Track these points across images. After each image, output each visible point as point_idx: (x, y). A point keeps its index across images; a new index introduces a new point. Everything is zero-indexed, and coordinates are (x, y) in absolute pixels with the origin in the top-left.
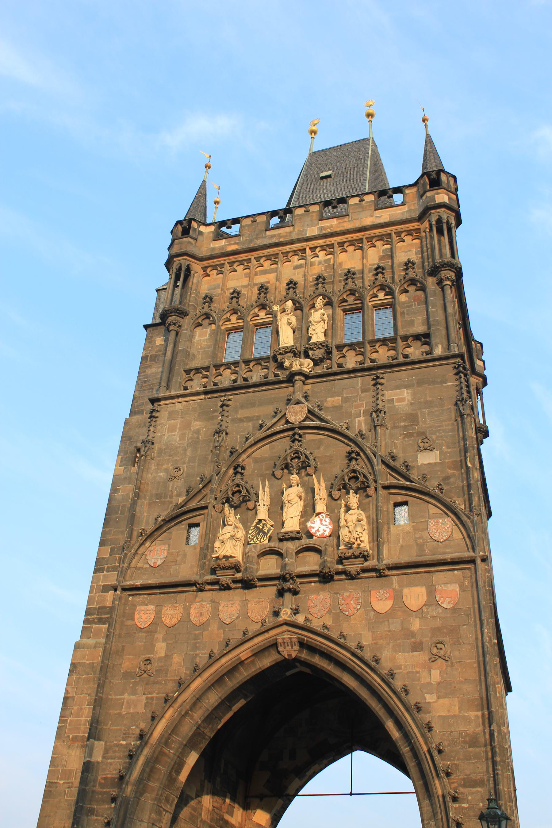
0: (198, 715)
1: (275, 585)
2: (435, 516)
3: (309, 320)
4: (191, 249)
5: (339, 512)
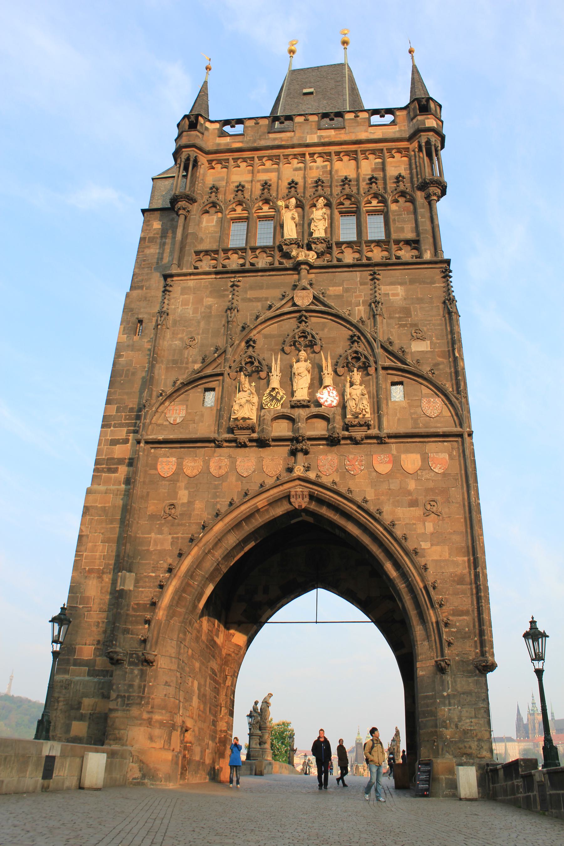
0: (219, 554)
2: (427, 396)
3: (312, 216)
4: (199, 142)
5: (345, 386)
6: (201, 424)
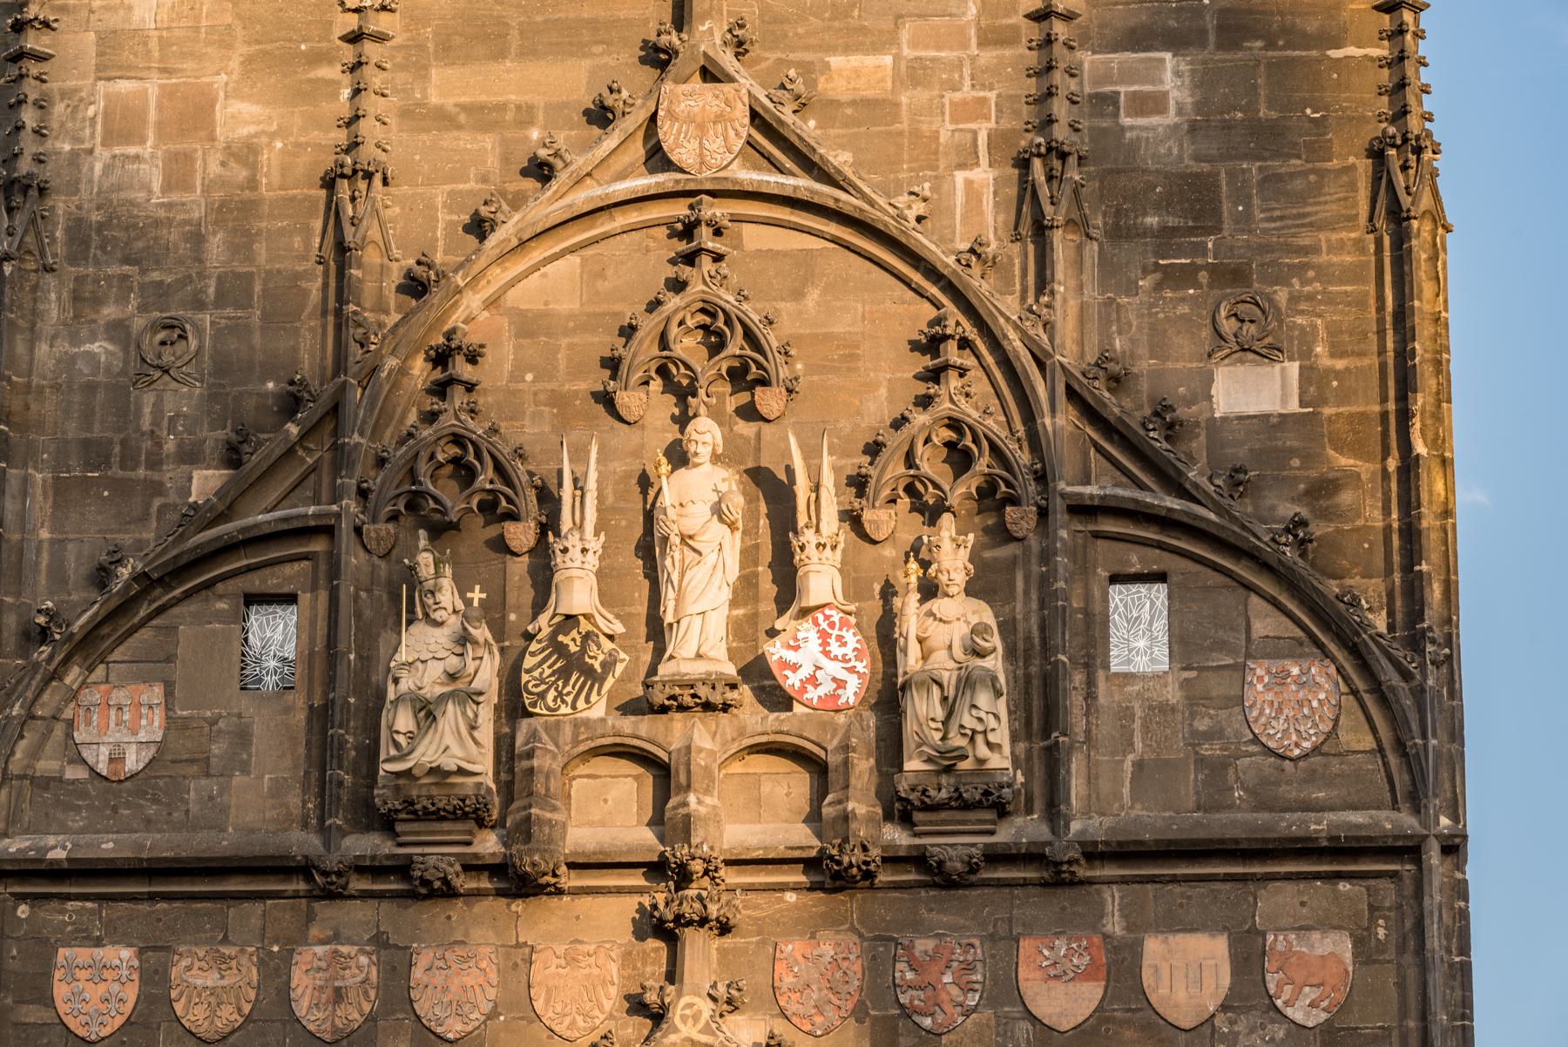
1: (632, 891)
2: (1274, 649)
6: (238, 779)
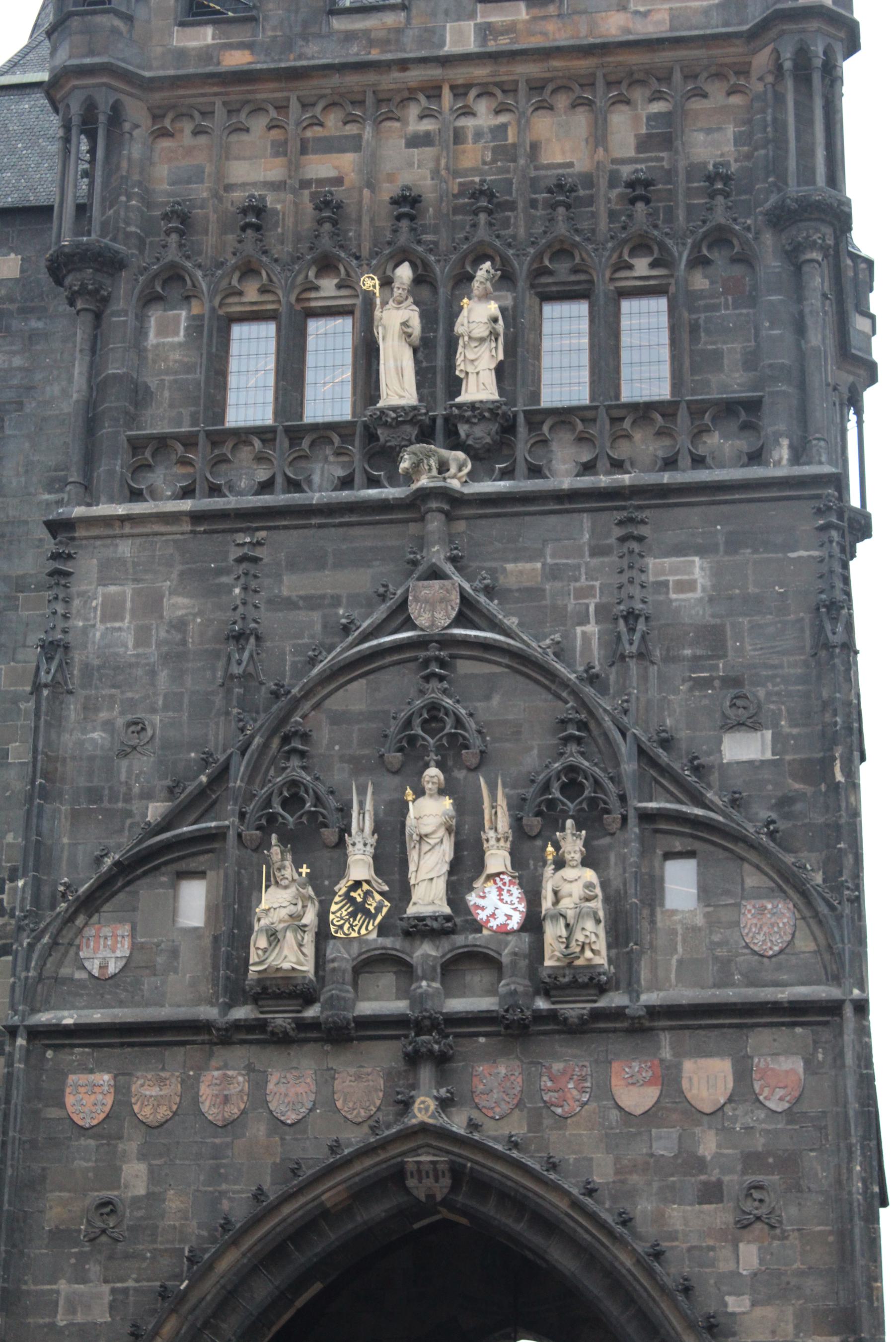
2: (758, 894)
4: (122, 55)
6: (172, 977)
